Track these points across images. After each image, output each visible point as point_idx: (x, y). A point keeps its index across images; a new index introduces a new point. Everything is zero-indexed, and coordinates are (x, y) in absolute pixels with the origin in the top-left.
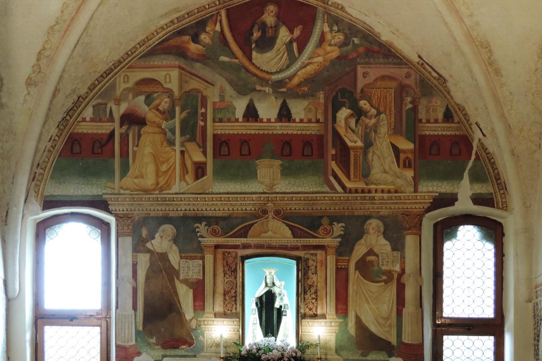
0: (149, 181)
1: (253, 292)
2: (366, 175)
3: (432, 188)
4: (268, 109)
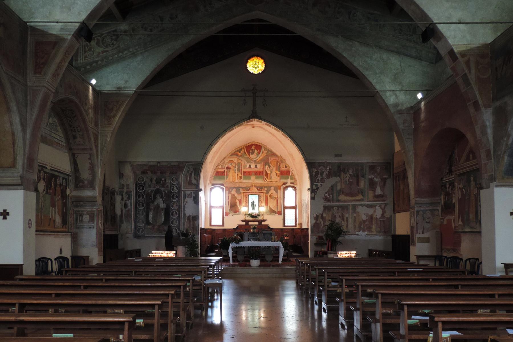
0: (231, 180)
1: (250, 201)
2: (271, 179)
4: (253, 166)
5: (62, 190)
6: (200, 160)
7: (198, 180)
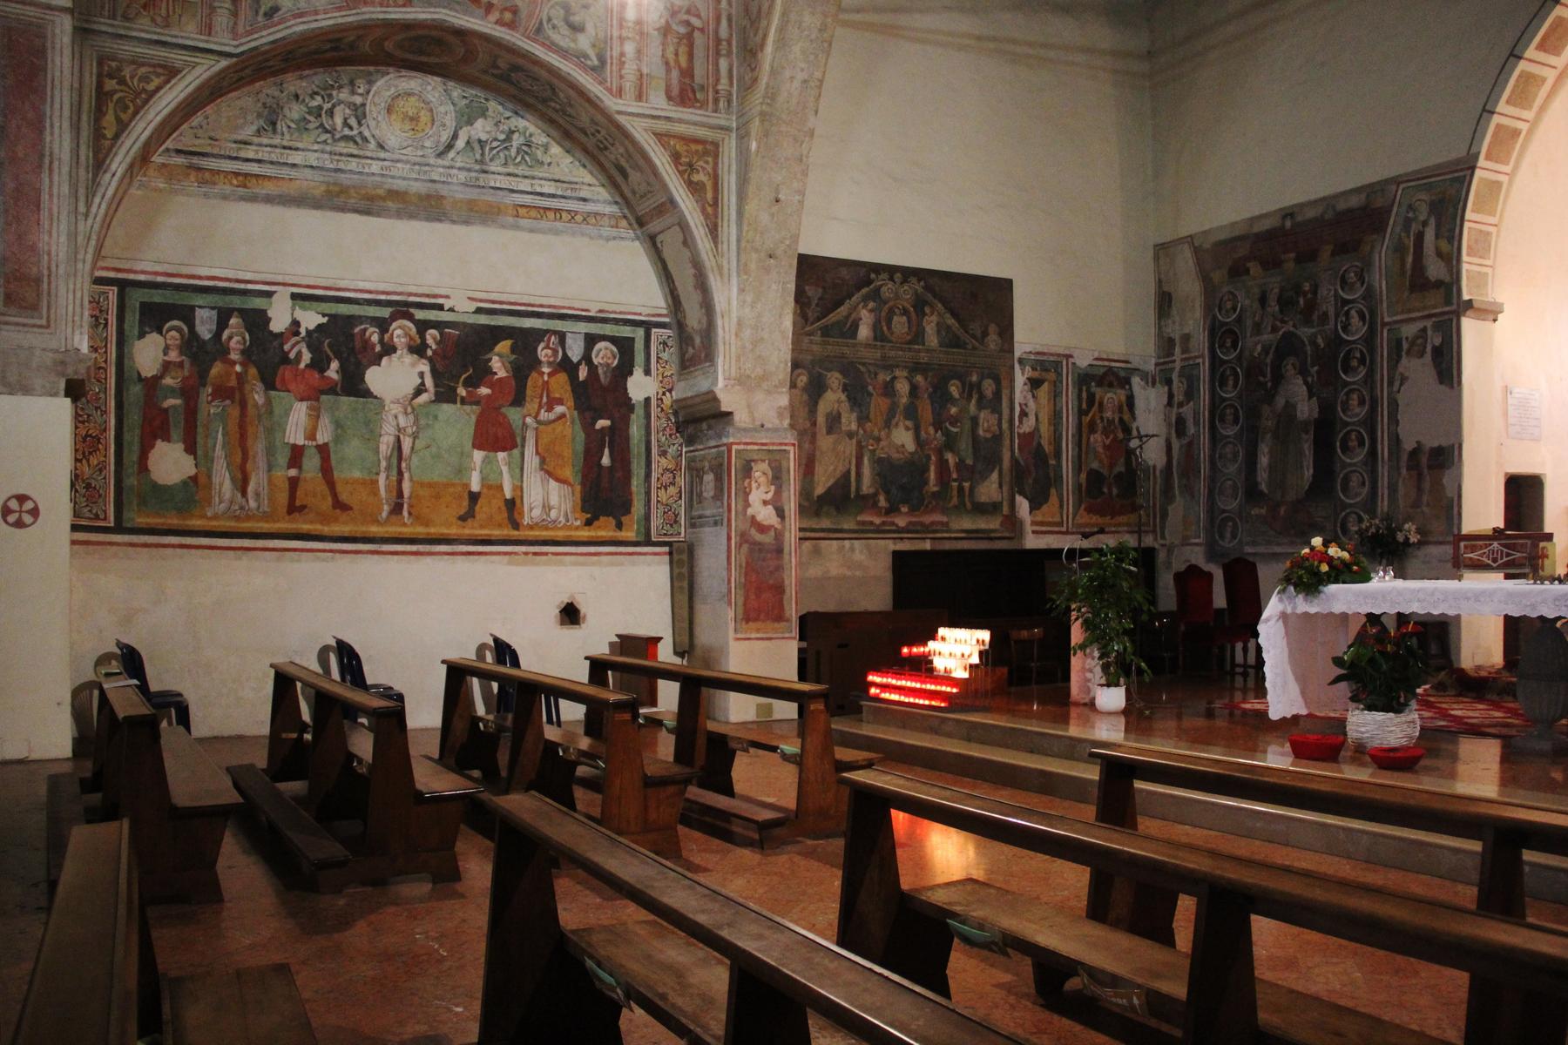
6: (1459, 152)
7: (1452, 260)
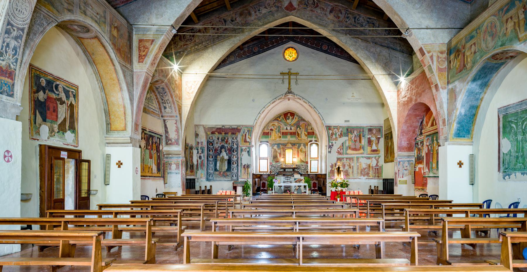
3: (310, 139)
4: (289, 128)
5: (157, 147)
